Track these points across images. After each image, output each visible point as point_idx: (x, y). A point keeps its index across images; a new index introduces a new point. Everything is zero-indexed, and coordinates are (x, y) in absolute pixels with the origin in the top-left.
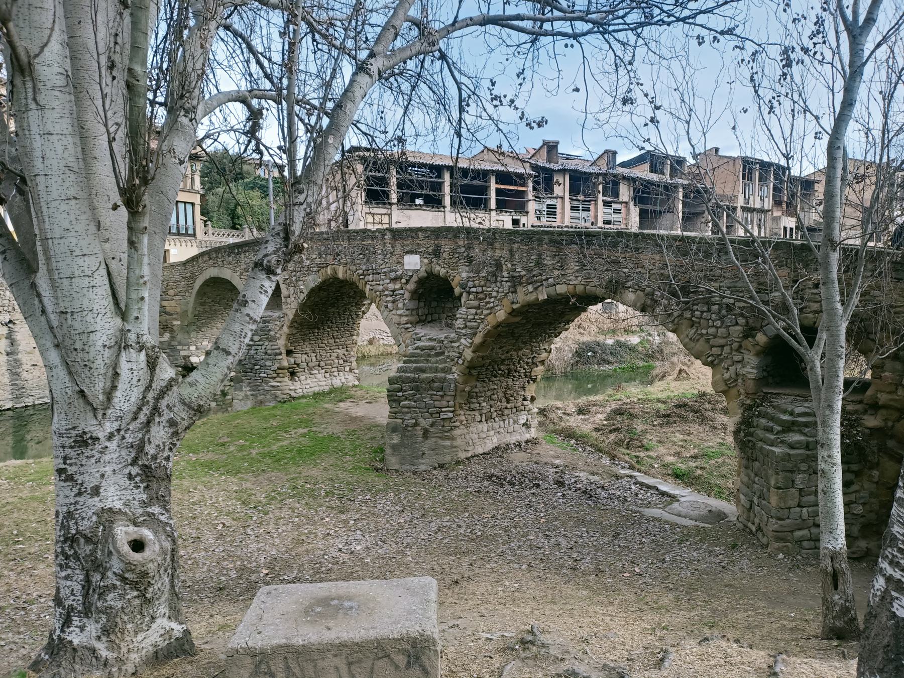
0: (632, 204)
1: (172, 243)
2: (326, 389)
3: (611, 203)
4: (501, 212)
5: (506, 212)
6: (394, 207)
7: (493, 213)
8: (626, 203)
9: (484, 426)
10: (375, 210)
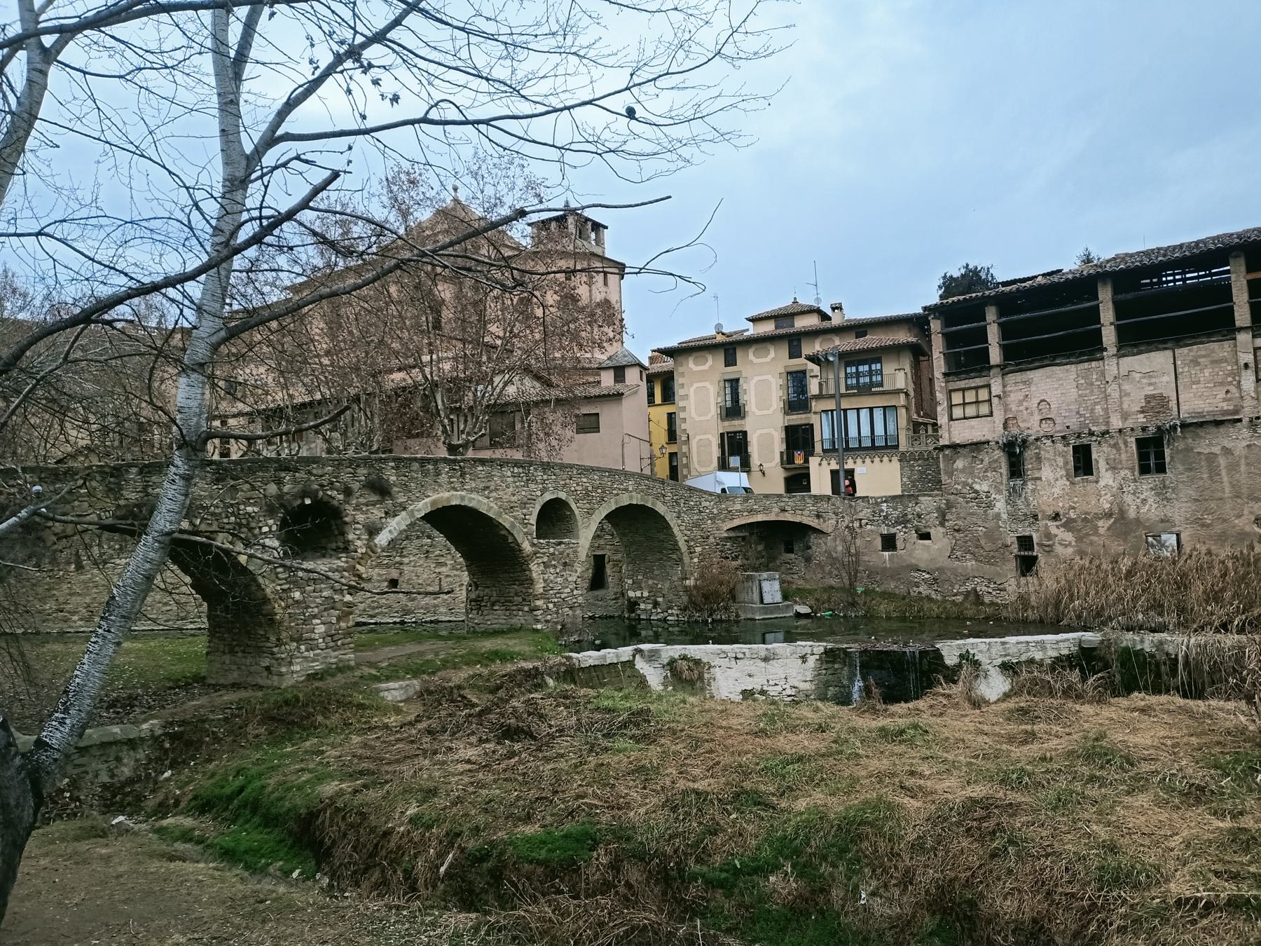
1: (859, 461)
2: (505, 628)
7: (1244, 338)
9: (227, 658)
10: (962, 384)
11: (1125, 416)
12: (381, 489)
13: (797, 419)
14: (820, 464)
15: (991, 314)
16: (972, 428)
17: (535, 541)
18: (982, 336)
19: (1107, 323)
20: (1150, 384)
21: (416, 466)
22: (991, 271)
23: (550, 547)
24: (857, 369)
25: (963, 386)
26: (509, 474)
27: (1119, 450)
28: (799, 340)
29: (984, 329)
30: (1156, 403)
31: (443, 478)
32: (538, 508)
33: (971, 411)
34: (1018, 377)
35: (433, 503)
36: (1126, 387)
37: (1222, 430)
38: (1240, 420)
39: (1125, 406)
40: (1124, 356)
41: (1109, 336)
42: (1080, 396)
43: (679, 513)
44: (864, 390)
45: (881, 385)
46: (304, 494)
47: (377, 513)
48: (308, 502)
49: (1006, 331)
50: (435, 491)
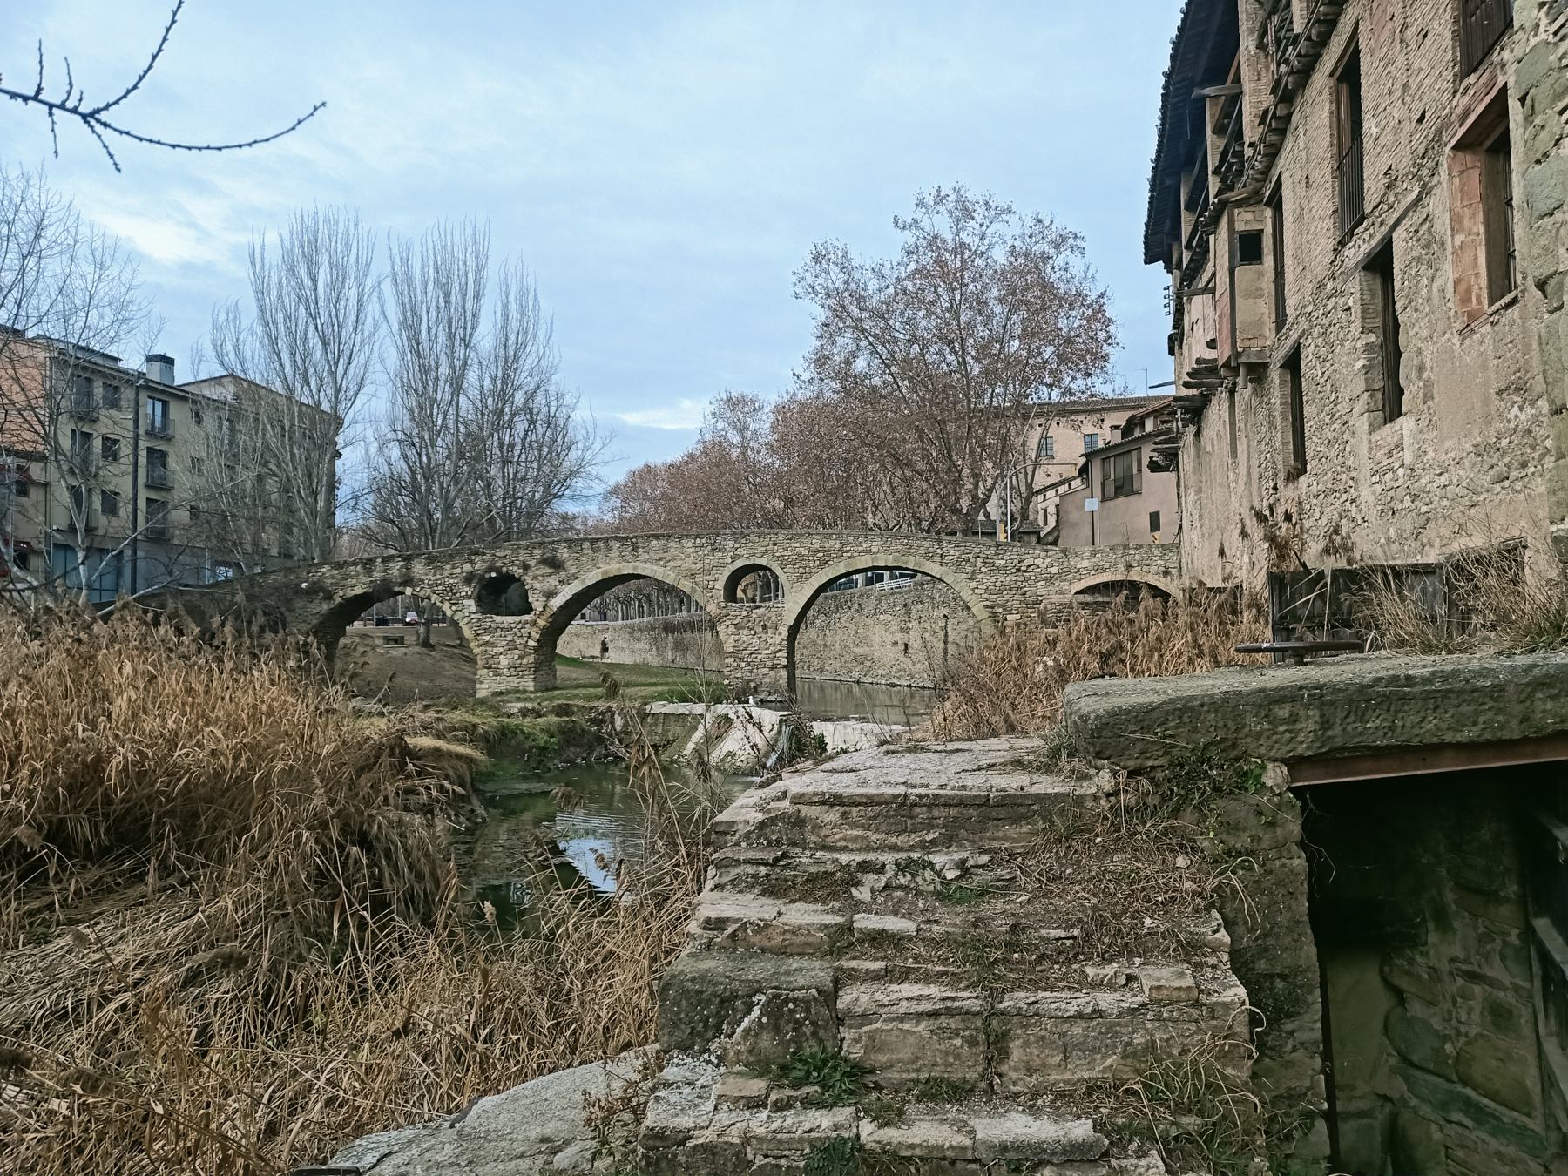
12: (555, 564)
17: (723, 605)
21: (586, 545)
23: (739, 612)
26: (690, 544)
31: (615, 553)
32: (727, 574)
35: (606, 572)
43: (973, 573)
46: (490, 570)
47: (553, 581)
48: (494, 575)
50: (606, 563)
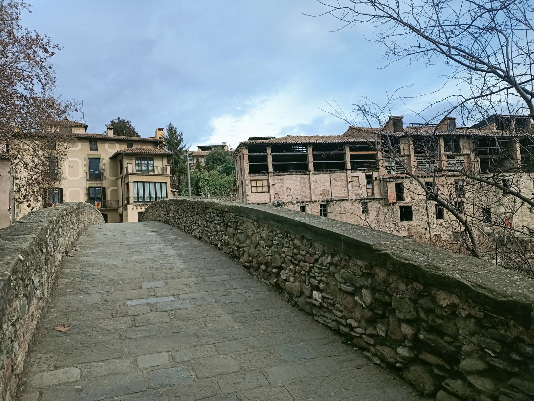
0: (473, 156)
3: (454, 155)
4: (356, 170)
5: (360, 170)
6: (270, 174)
7: (349, 172)
8: (468, 155)
10: (256, 178)
11: (316, 196)
13: (94, 184)
14: (133, 209)
15: (269, 151)
16: (261, 196)
18: (265, 159)
19: (311, 161)
20: (323, 185)
22: (130, 123)
24: (141, 162)
25: (256, 179)
27: (315, 208)
28: (97, 142)
29: (266, 156)
30: (325, 192)
33: (260, 189)
34: (279, 177)
36: (316, 185)
37: (343, 202)
38: (348, 200)
39: (316, 192)
40: (316, 174)
41: (311, 166)
42: (301, 187)
44: (146, 173)
45: (154, 171)
49: (274, 159)
